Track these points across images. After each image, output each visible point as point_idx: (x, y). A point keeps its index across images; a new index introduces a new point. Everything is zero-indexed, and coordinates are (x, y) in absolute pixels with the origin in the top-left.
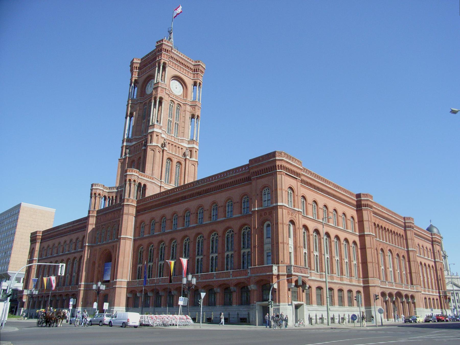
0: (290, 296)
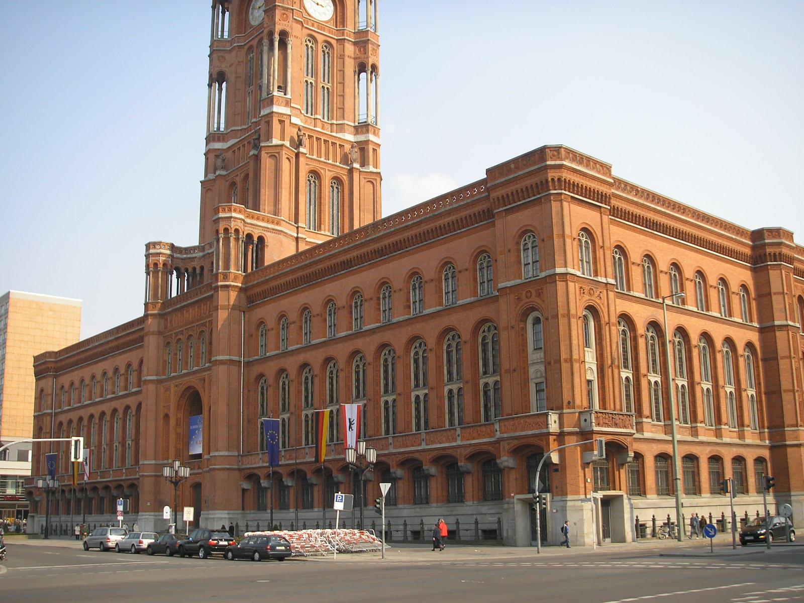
0: (589, 481)
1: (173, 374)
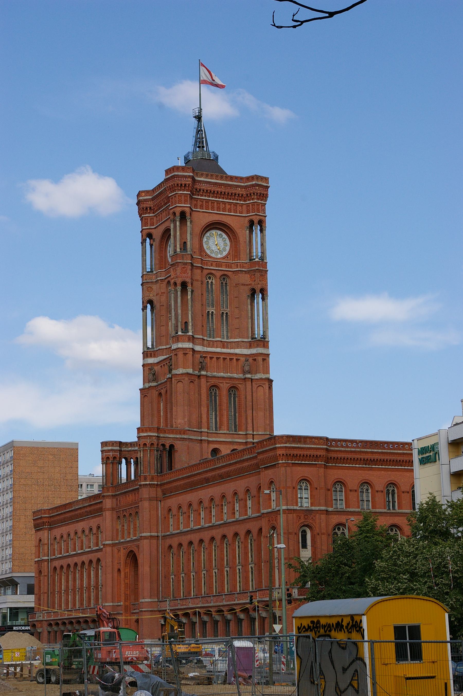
1: (122, 540)
